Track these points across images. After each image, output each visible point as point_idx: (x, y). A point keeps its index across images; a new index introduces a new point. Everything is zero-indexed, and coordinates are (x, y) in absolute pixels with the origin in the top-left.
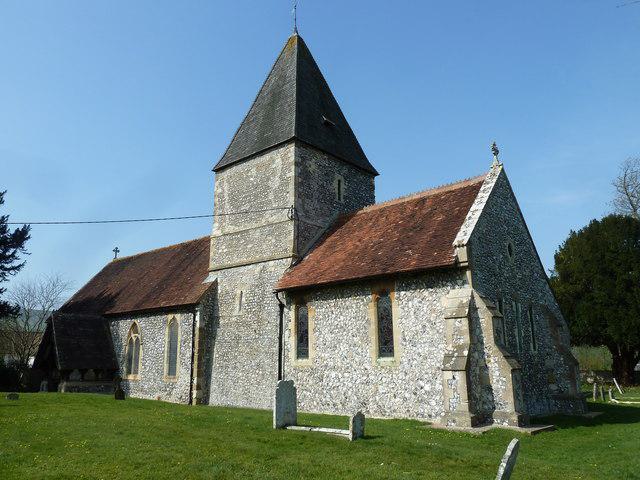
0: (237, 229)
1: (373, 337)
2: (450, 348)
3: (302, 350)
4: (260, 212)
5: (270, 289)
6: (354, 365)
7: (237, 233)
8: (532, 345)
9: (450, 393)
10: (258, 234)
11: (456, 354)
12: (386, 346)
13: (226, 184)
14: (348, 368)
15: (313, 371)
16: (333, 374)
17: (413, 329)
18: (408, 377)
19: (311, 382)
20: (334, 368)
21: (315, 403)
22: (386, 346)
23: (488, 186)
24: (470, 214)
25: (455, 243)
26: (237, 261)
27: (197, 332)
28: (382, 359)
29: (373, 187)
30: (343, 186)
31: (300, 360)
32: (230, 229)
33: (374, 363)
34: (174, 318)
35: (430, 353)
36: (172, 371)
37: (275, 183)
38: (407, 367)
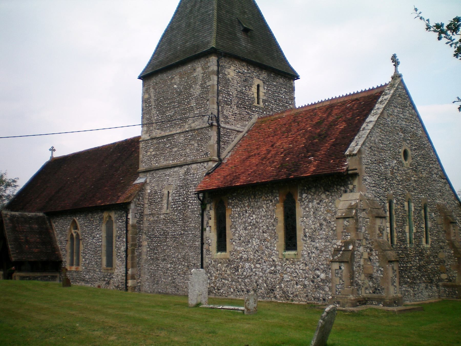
0: (163, 134)
1: (281, 234)
2: (339, 243)
3: (222, 246)
4: (184, 120)
5: (193, 190)
6: (265, 258)
7: (163, 137)
8: (424, 240)
9: (337, 280)
10: (182, 139)
11: (343, 248)
12: (291, 242)
13: (152, 90)
14: (259, 260)
15: (229, 262)
16: (247, 265)
17: (313, 226)
18: (308, 267)
19: (228, 272)
20: (247, 260)
21: (232, 290)
22: (291, 242)
23: (385, 97)
24: (364, 125)
25: (347, 153)
26: (163, 163)
27: (130, 228)
29: (293, 89)
30: (261, 89)
31: (219, 253)
32: (158, 133)
33: (280, 256)
35: (326, 247)
37: (197, 91)
38: (307, 259)
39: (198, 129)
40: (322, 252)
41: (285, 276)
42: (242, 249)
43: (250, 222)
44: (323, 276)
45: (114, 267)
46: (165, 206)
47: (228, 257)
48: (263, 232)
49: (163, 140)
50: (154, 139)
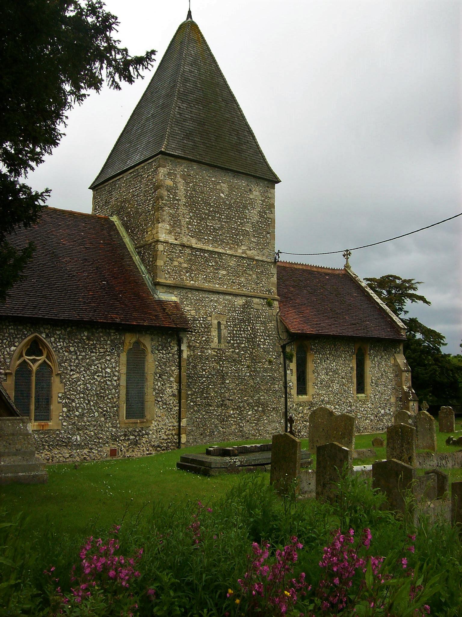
0: (200, 246)
3: (302, 389)
10: (232, 263)
28: (359, 395)
33: (355, 398)
34: (137, 343)
36: (136, 409)
38: (373, 400)
39: (257, 260)
40: (382, 394)
41: (359, 414)
42: (324, 392)
43: (332, 369)
44: (383, 411)
45: (148, 417)
46: (216, 340)
47: (311, 400)
48: (342, 378)
49: (202, 254)
50: (188, 247)
